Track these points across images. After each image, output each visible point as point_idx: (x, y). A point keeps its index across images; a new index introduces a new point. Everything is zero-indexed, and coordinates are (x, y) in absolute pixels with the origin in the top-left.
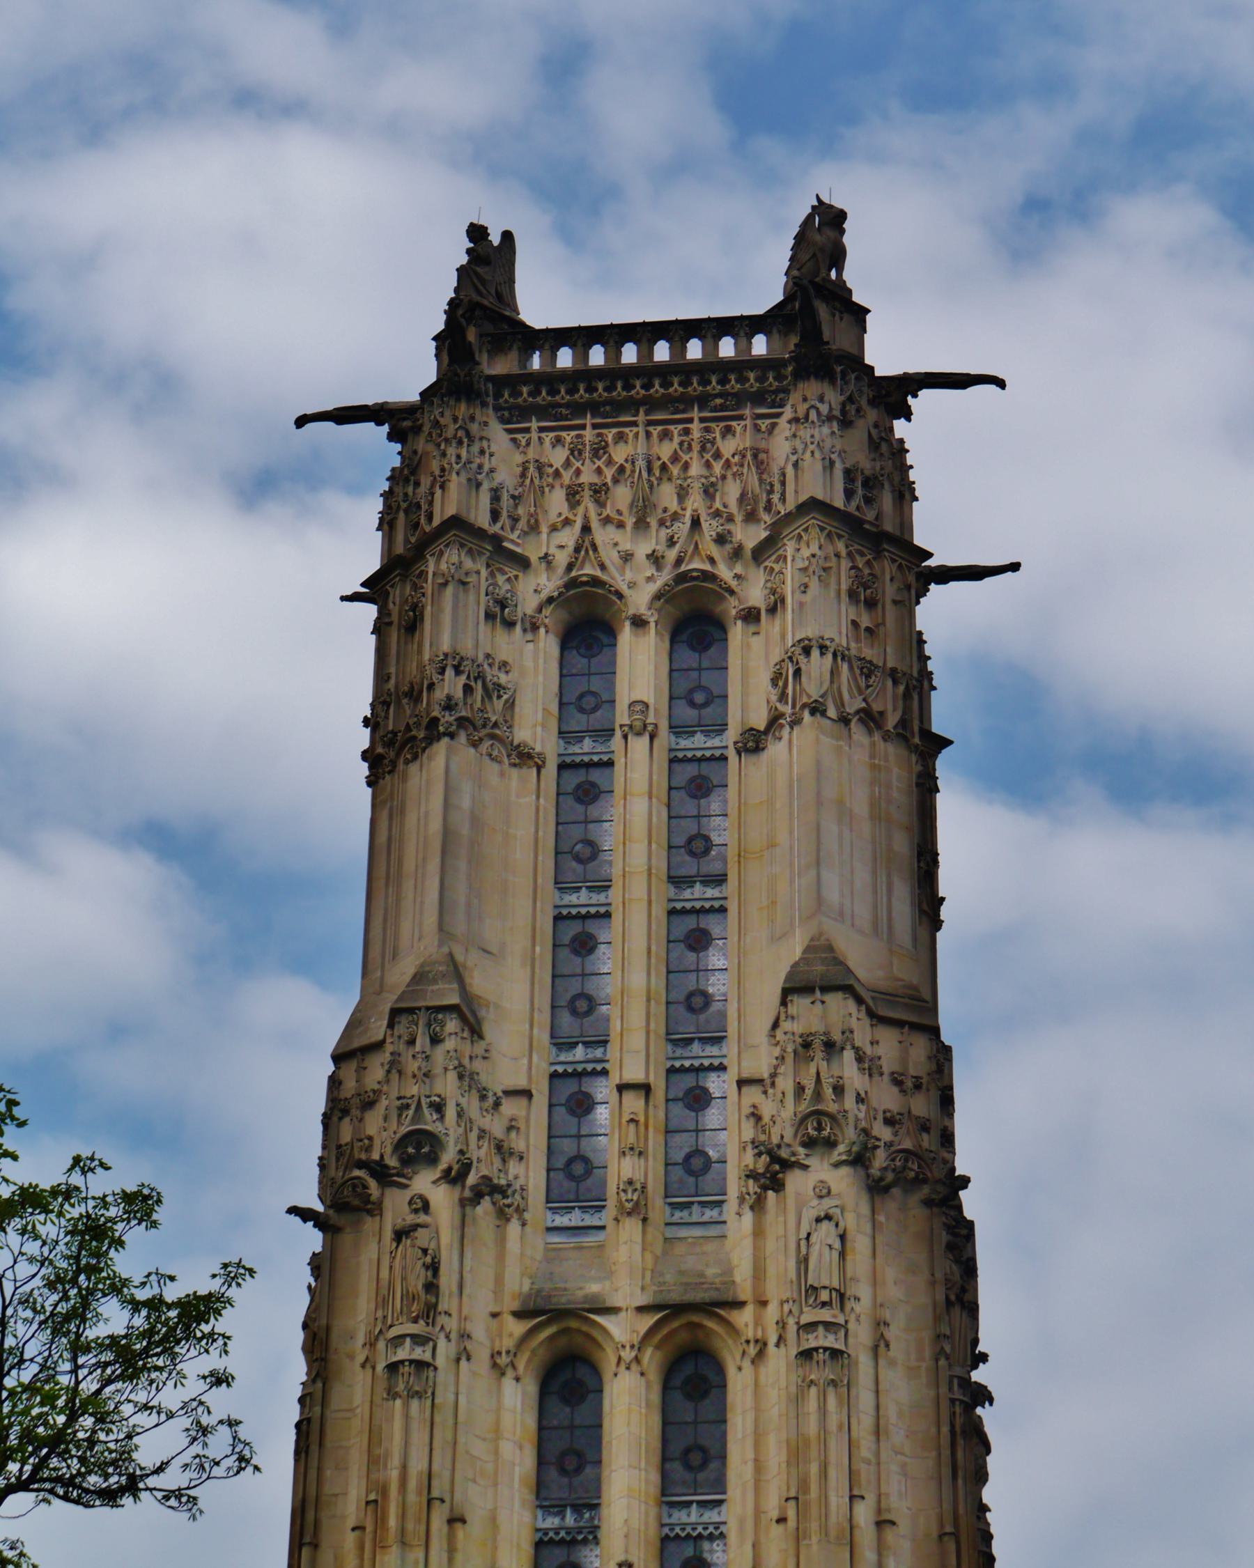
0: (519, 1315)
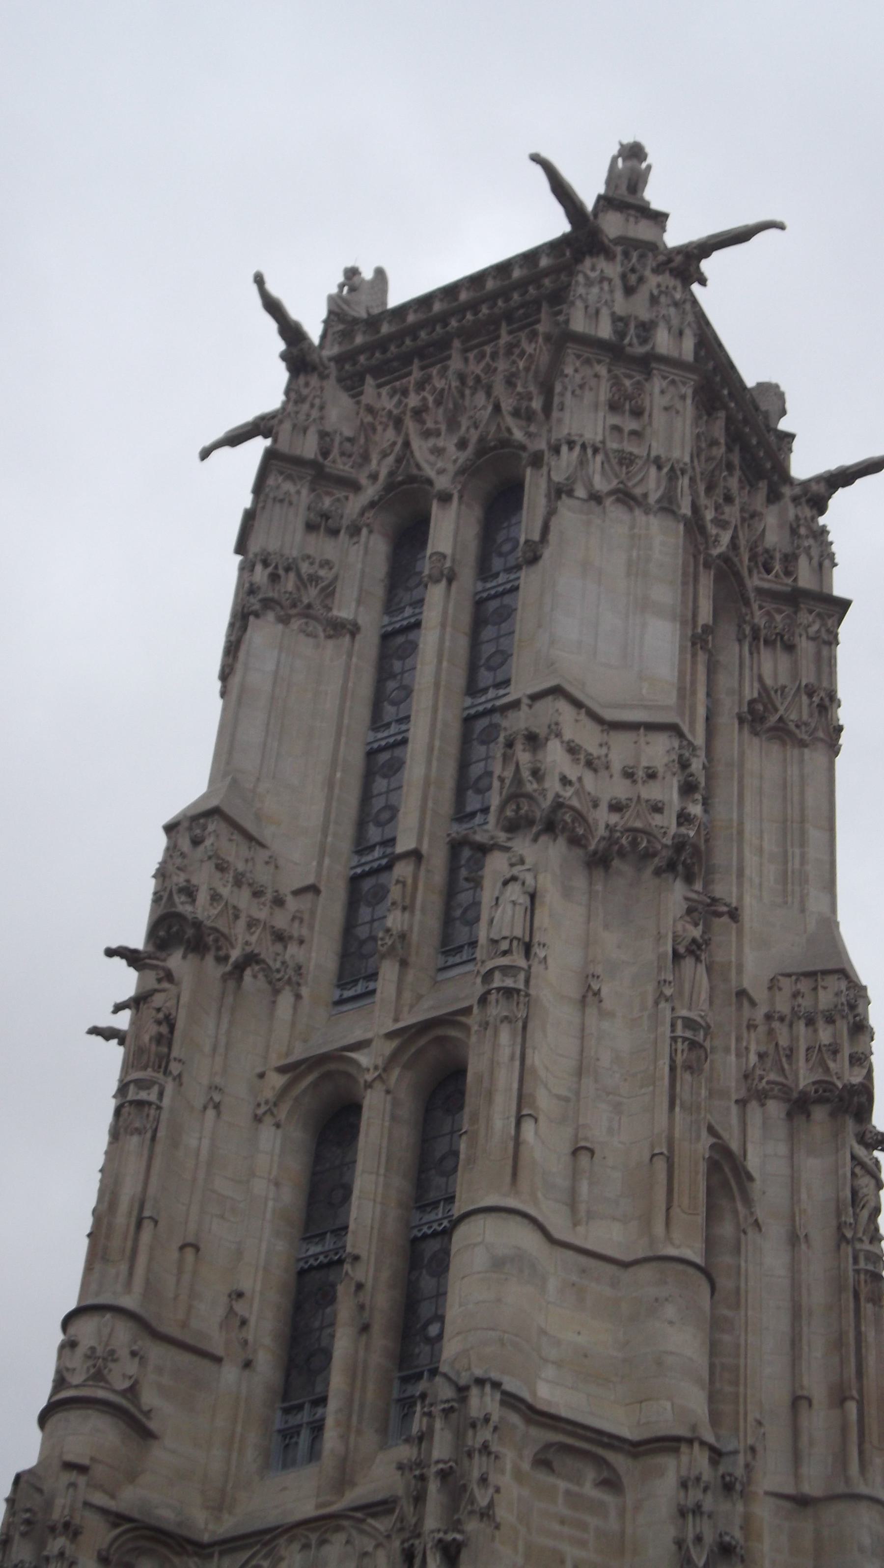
0: (282, 1070)
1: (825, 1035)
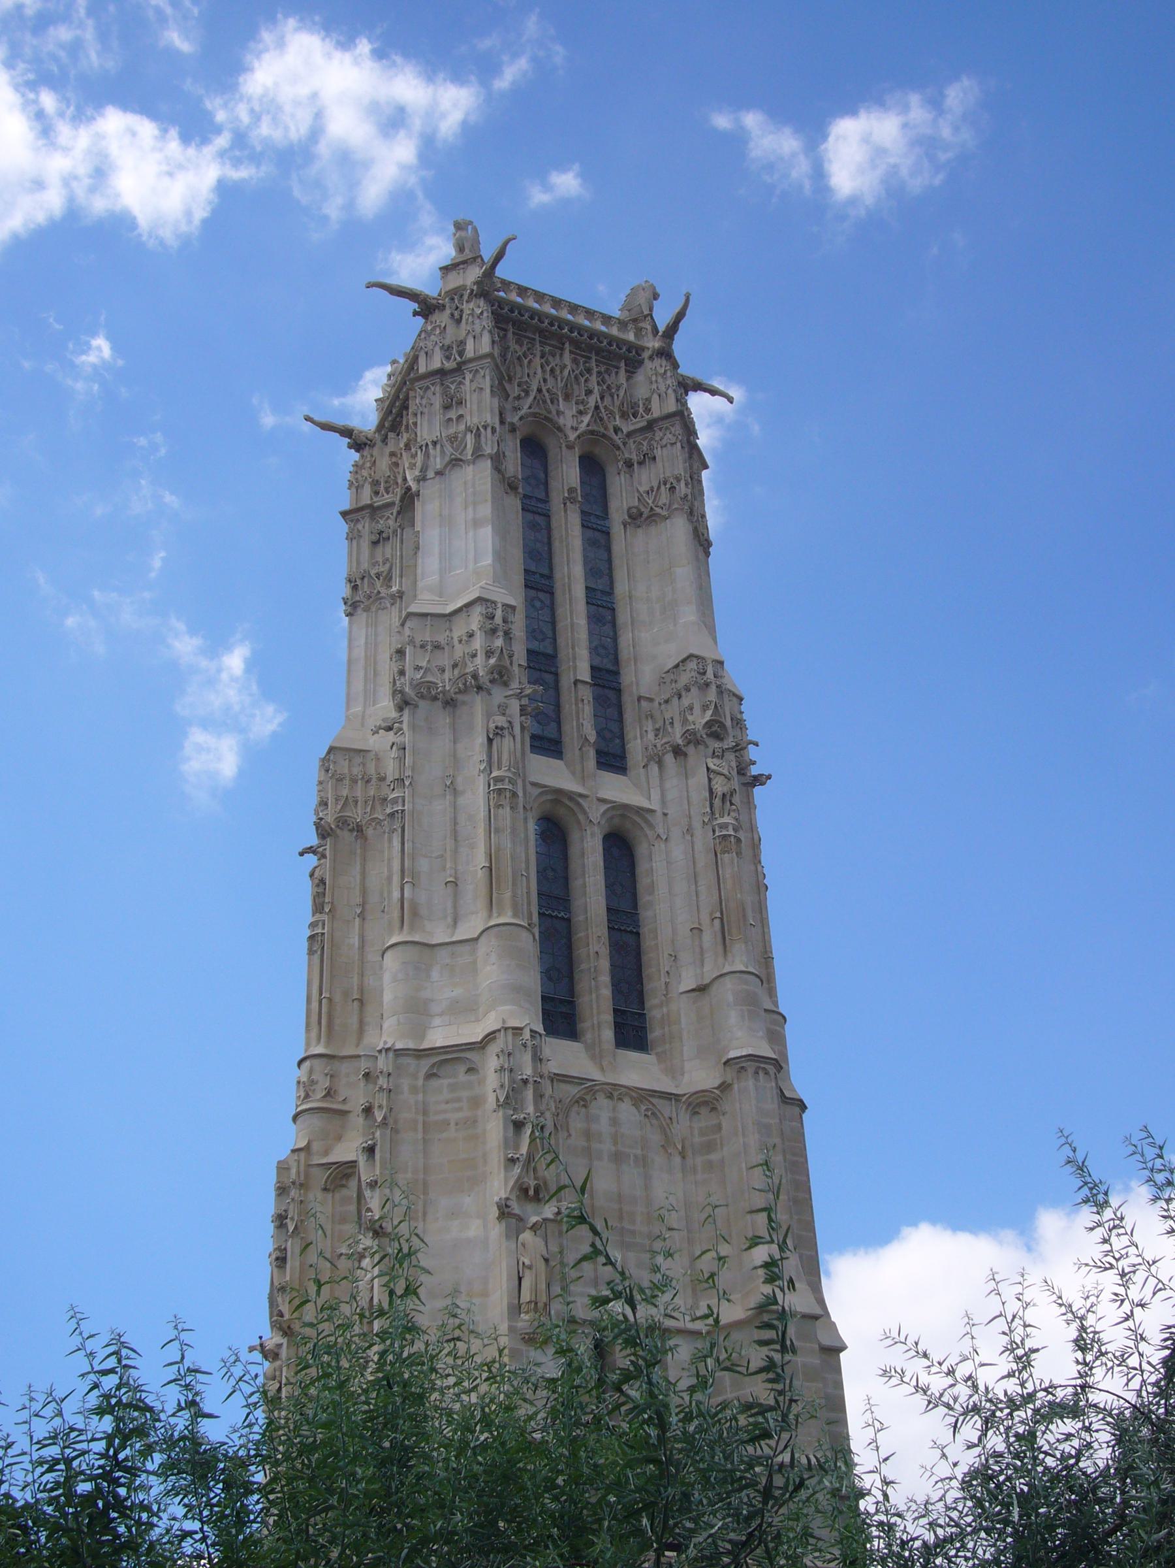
1: (686, 702)
